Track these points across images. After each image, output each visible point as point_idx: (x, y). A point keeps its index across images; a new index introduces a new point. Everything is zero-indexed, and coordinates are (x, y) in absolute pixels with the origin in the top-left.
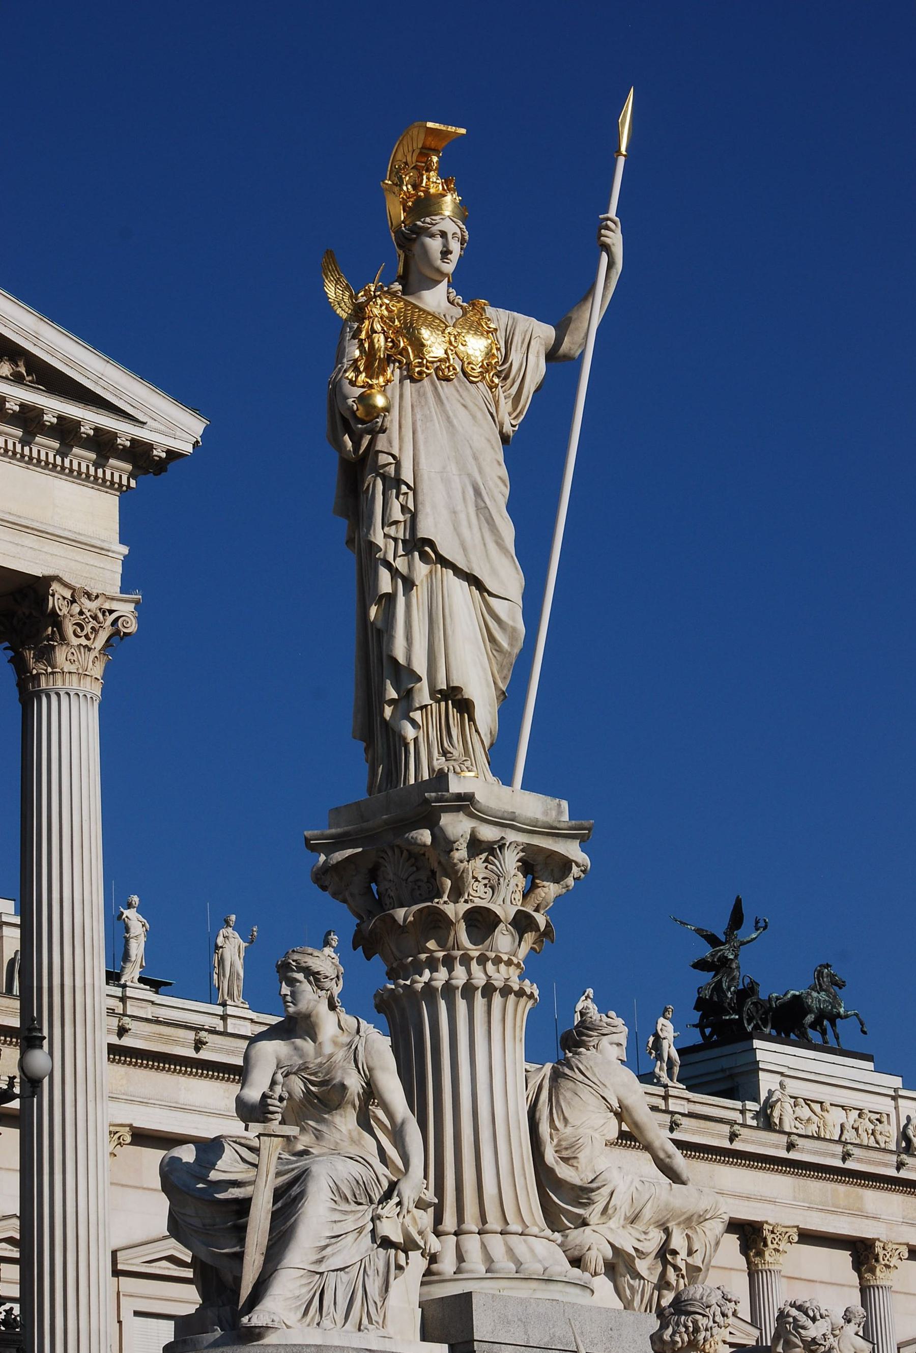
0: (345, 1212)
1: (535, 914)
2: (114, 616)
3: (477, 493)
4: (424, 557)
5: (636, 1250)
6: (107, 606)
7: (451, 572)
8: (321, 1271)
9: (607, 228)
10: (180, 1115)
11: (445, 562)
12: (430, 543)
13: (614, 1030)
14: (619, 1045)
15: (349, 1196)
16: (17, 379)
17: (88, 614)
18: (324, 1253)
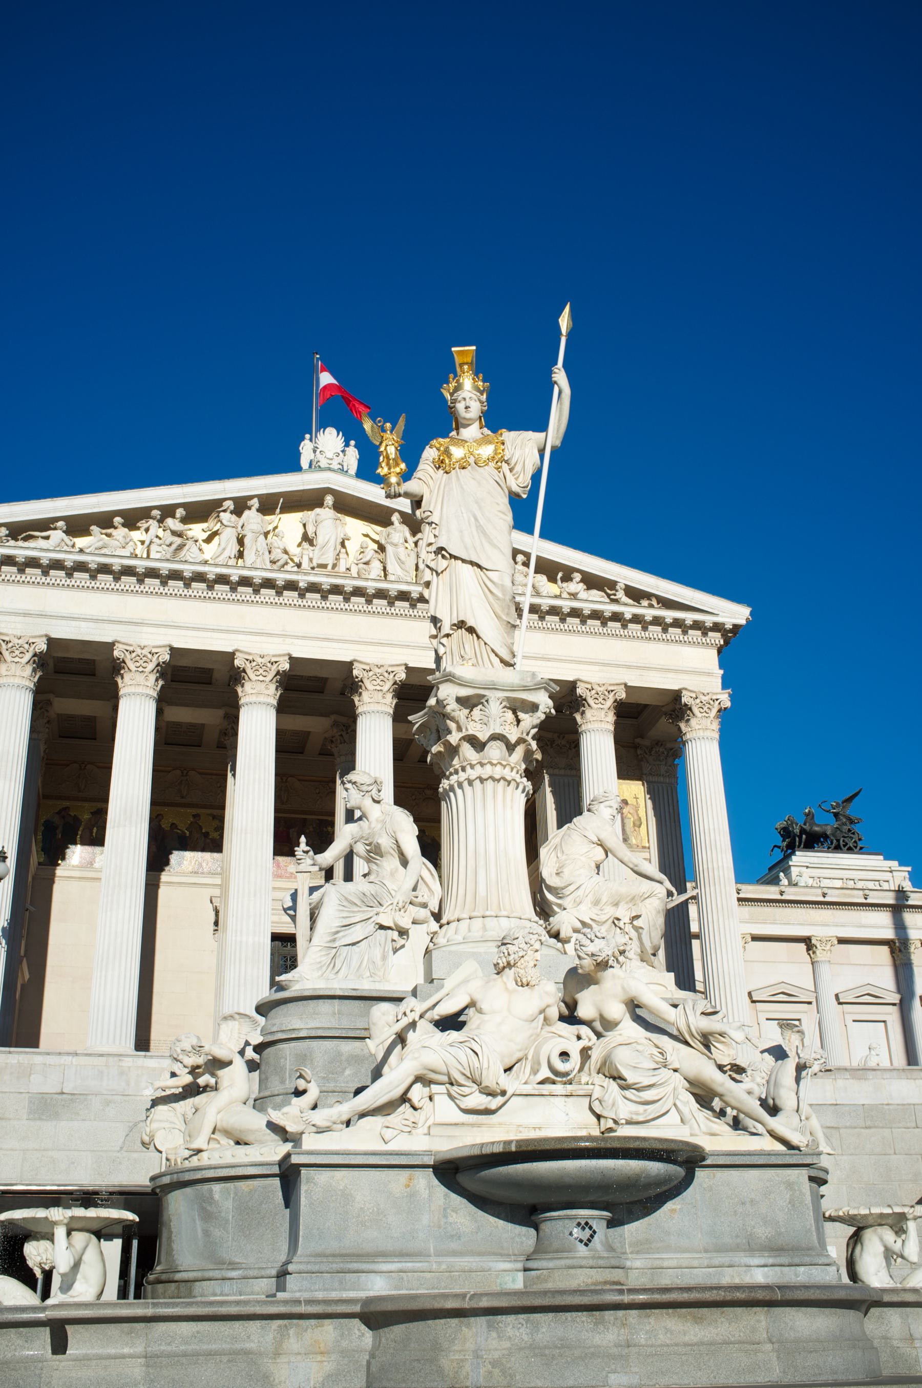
0: (353, 912)
1: (526, 738)
2: (719, 701)
3: (476, 519)
4: (443, 557)
5: (591, 919)
6: (714, 697)
7: (460, 562)
8: (334, 946)
9: (555, 373)
10: (863, 929)
11: (456, 558)
12: (442, 549)
13: (606, 799)
14: (611, 807)
15: (359, 903)
16: (651, 606)
17: (705, 702)
18: (336, 936)
